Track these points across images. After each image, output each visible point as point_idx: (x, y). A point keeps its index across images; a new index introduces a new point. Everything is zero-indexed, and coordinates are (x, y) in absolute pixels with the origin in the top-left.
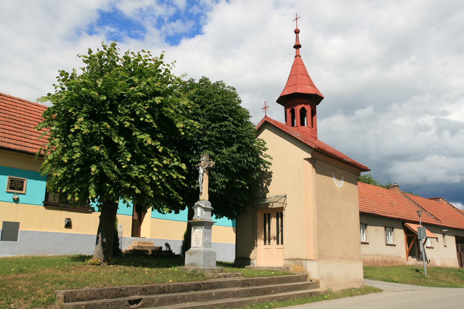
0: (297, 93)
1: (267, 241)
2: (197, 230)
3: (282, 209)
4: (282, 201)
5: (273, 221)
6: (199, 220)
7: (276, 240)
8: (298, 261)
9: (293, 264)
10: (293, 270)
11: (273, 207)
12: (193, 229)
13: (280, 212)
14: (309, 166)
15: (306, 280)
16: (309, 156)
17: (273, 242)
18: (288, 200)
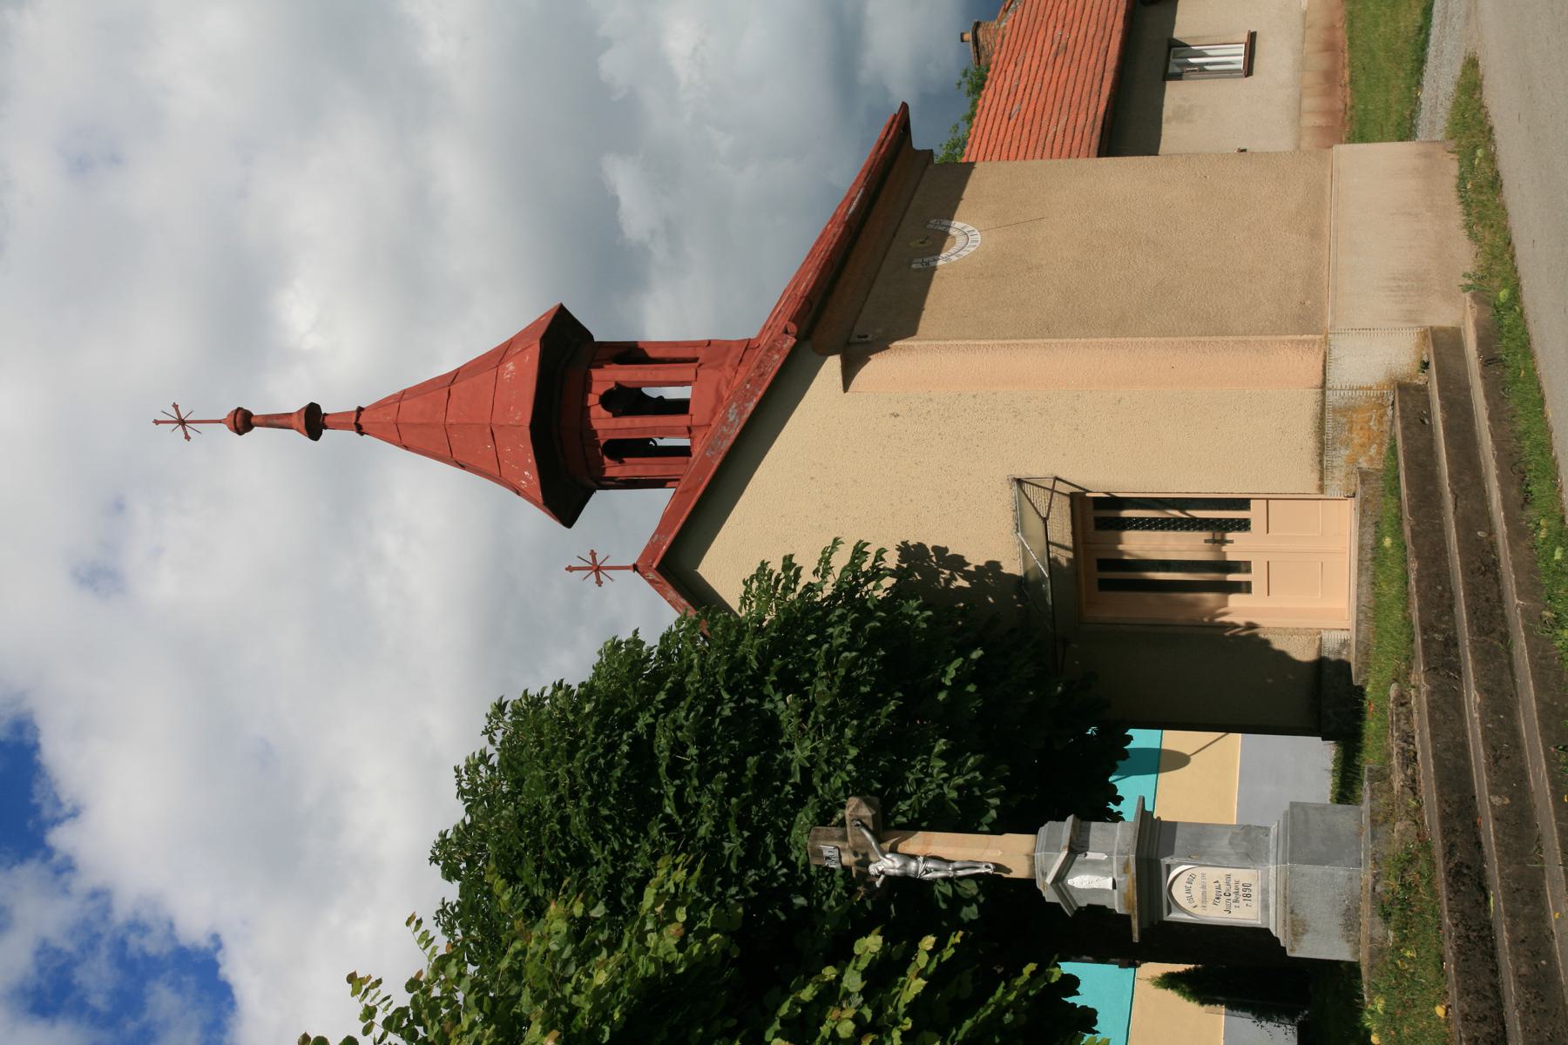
0: (534, 427)
1: (1232, 577)
2: (1179, 893)
3: (1078, 500)
4: (1041, 499)
5: (1136, 544)
6: (1128, 881)
7: (1229, 536)
8: (1329, 426)
9: (1344, 452)
10: (1373, 451)
11: (1069, 542)
12: (1176, 916)
13: (1091, 514)
14: (877, 367)
15: (1422, 390)
16: (833, 364)
17: (1237, 547)
18: (1037, 468)
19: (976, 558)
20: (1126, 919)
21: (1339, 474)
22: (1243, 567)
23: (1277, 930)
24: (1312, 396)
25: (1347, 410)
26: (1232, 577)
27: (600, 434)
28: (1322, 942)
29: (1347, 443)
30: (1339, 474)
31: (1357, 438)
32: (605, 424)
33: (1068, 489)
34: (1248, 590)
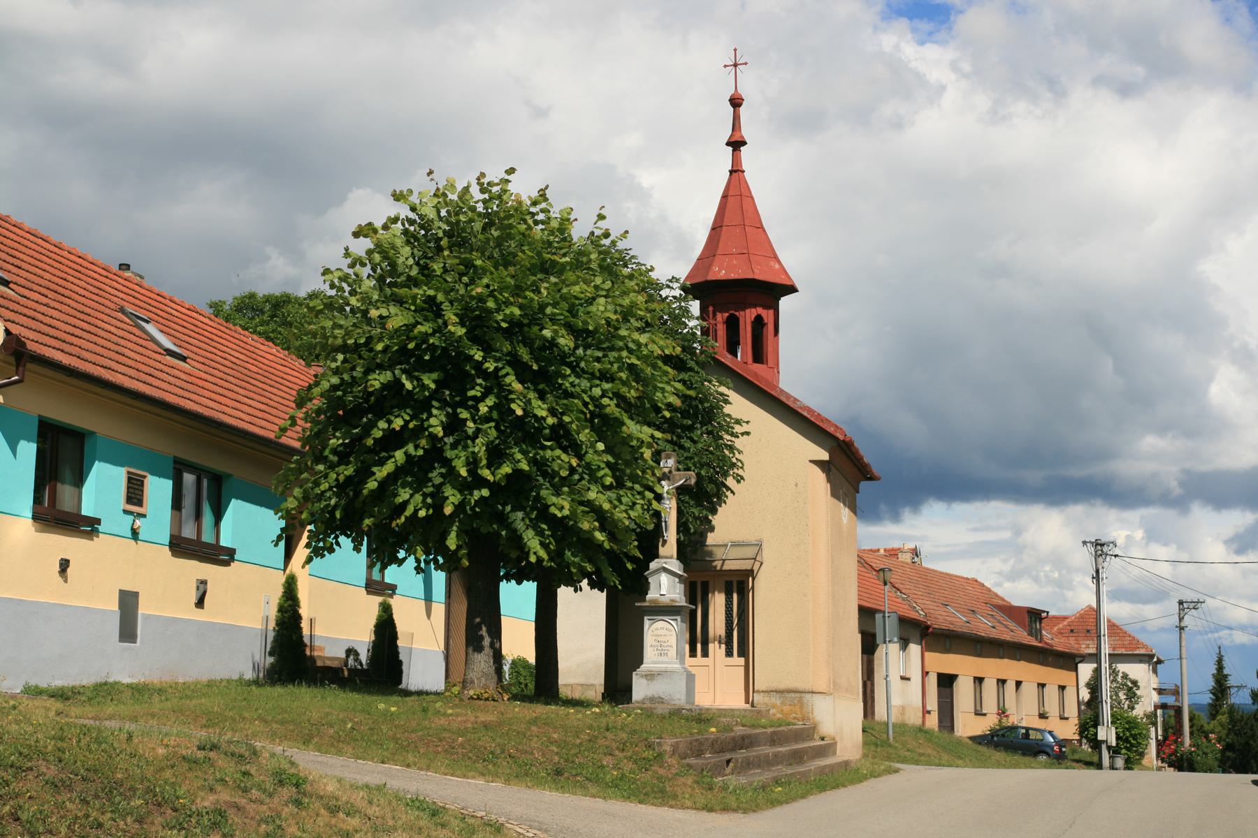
0: (754, 280)
1: (699, 646)
2: (660, 624)
3: (750, 573)
4: (750, 552)
5: (718, 601)
6: (665, 601)
7: (723, 646)
8: (793, 695)
9: (778, 702)
10: (779, 716)
11: (726, 567)
12: (647, 623)
13: (735, 579)
14: (820, 476)
15: (812, 739)
16: (824, 456)
17: (717, 650)
18: (766, 554)
19: (716, 520)
20: (644, 600)
21: (766, 700)
22: (705, 654)
23: (644, 667)
24: (808, 687)
25: (801, 703)
26: (699, 646)
27: (742, 313)
28: (641, 689)
29: (783, 703)
30: (766, 700)
31: (786, 708)
32: (747, 317)
33: (756, 569)
34: (691, 656)
